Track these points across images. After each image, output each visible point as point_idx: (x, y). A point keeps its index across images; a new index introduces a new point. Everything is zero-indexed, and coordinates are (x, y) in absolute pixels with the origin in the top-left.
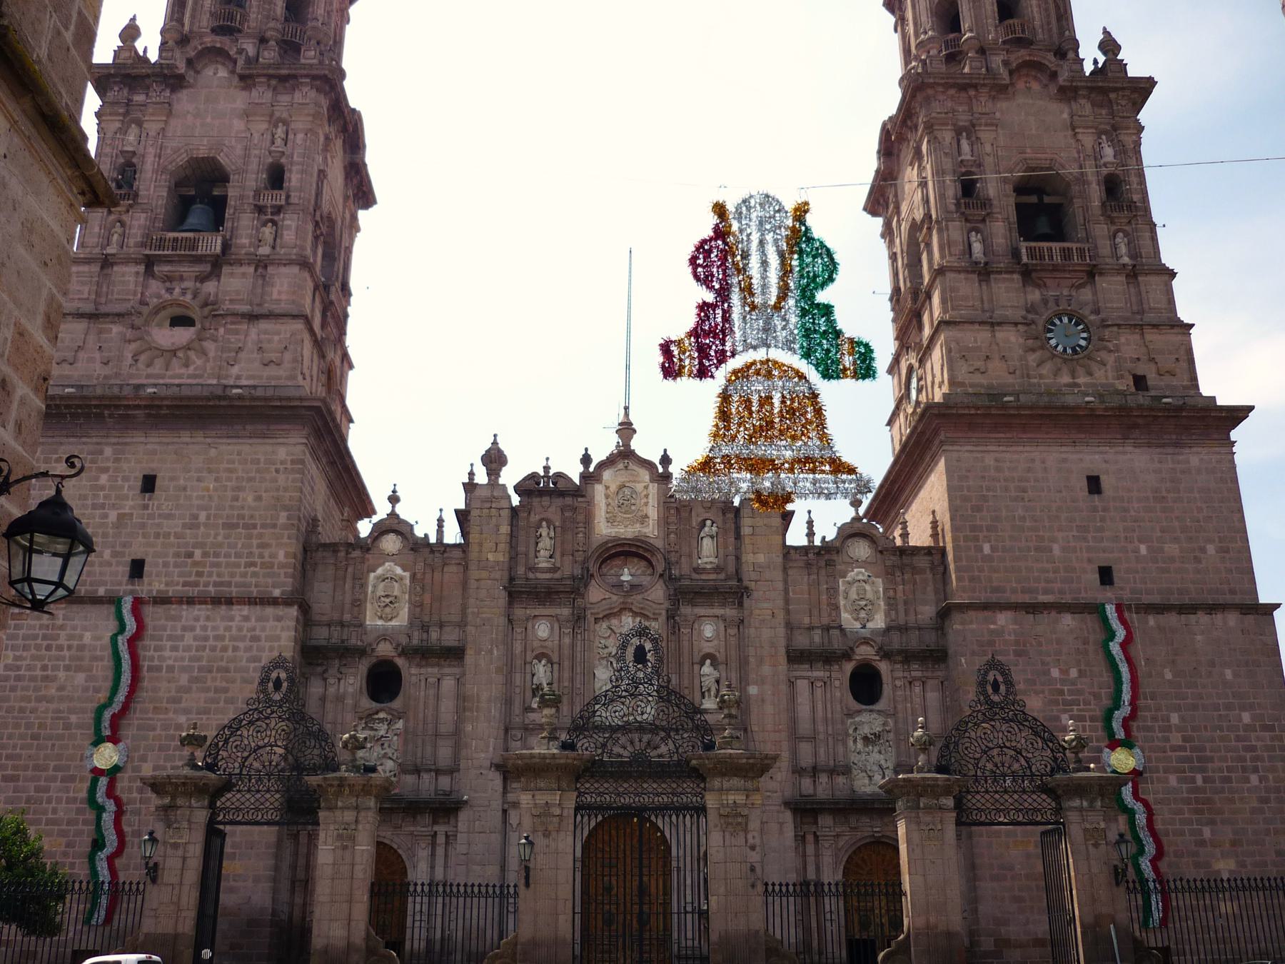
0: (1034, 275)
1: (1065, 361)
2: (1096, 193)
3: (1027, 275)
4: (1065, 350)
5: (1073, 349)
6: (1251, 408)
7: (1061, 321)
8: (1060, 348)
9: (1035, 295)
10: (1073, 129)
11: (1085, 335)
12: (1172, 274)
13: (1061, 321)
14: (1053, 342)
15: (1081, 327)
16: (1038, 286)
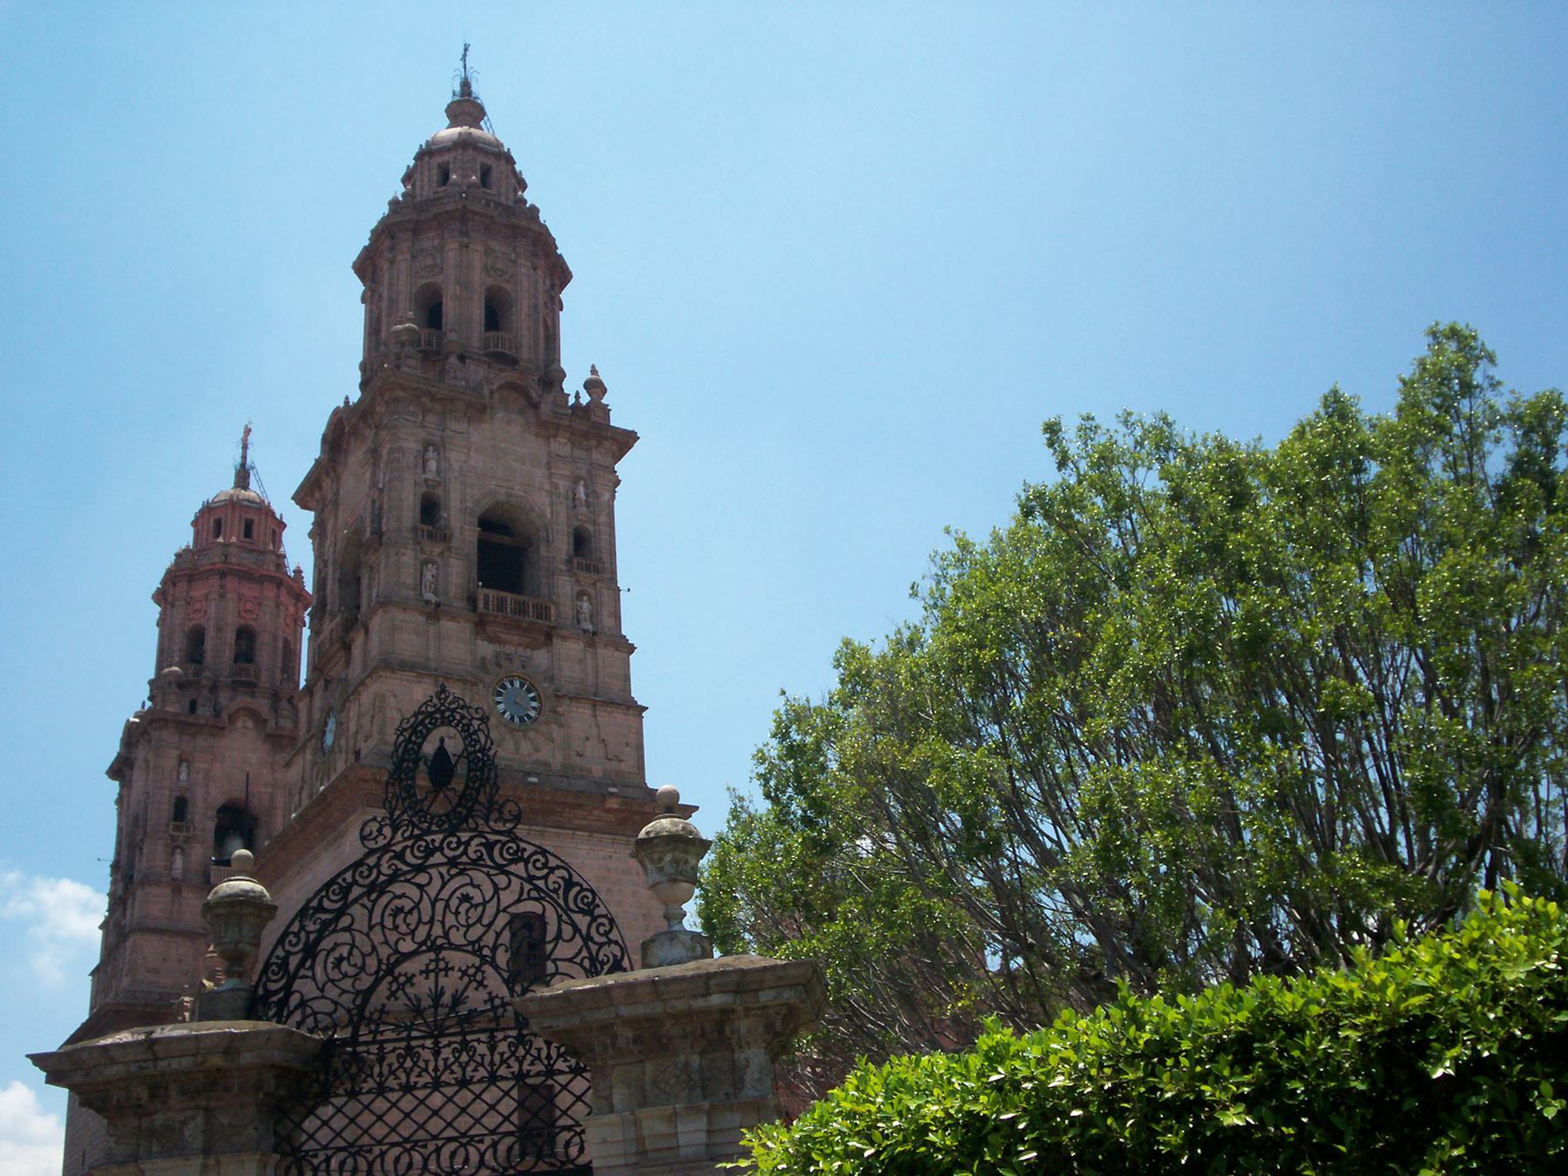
0: (488, 628)
1: (512, 731)
2: (562, 546)
3: (481, 625)
4: (512, 718)
5: (522, 720)
6: (696, 808)
7: (512, 685)
8: (507, 715)
9: (486, 649)
10: (549, 466)
11: (534, 704)
12: (632, 649)
13: (512, 685)
14: (501, 707)
15: (532, 695)
16: (491, 640)
